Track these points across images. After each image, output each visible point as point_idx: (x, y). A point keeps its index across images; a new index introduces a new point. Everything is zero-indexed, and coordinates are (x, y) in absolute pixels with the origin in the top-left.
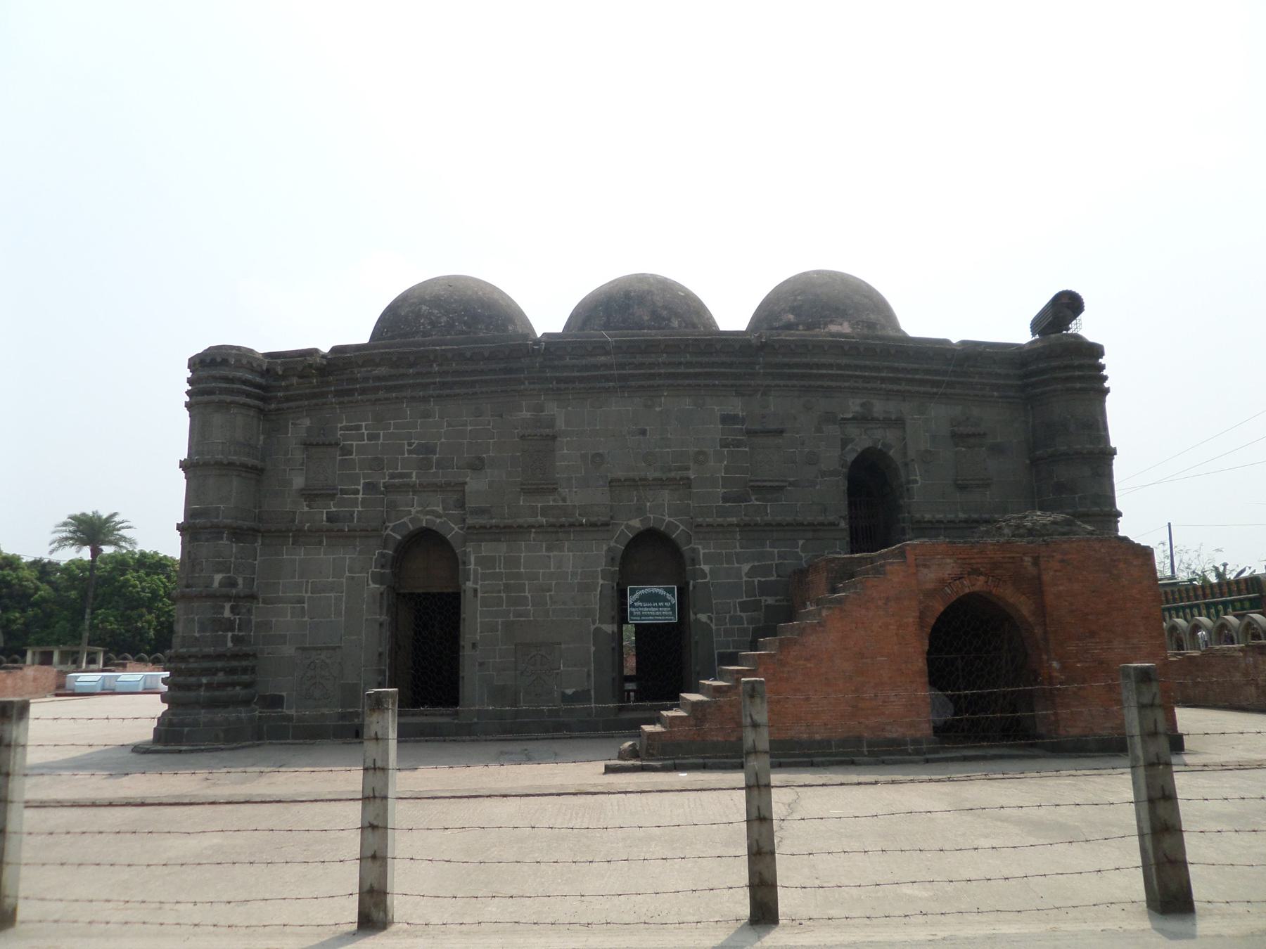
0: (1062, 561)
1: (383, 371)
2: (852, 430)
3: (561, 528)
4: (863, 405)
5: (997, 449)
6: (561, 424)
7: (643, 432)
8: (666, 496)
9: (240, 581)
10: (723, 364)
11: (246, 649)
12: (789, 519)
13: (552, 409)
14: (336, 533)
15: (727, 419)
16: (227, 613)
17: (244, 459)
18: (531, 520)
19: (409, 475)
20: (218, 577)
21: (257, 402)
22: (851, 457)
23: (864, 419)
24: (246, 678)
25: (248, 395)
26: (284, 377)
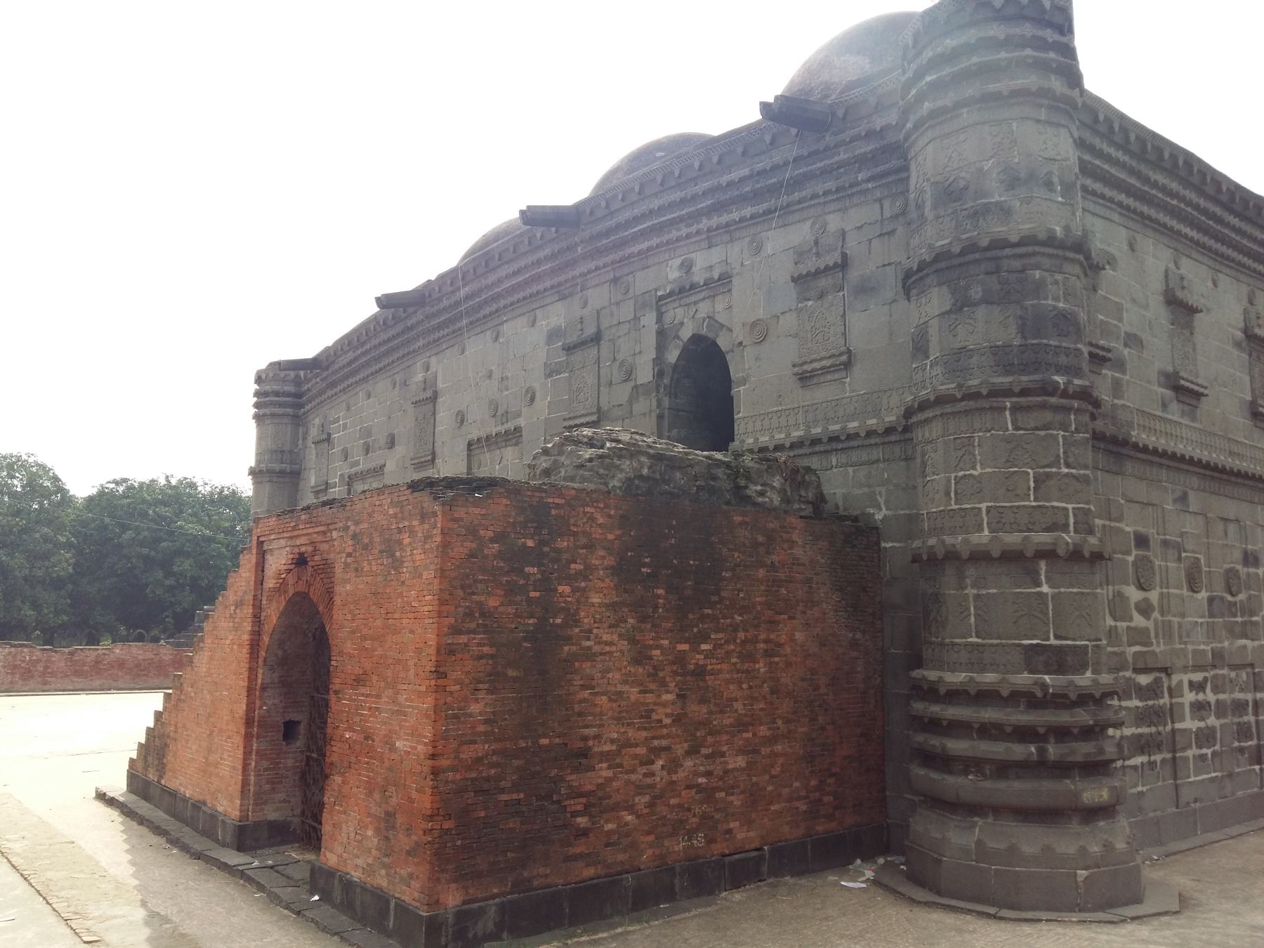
0: (354, 537)
1: (351, 355)
2: (675, 313)
4: (682, 264)
5: (865, 289)
8: (510, 453)
13: (433, 360)
15: (553, 335)
21: (289, 411)
22: (673, 356)
23: (684, 291)
25: (281, 405)
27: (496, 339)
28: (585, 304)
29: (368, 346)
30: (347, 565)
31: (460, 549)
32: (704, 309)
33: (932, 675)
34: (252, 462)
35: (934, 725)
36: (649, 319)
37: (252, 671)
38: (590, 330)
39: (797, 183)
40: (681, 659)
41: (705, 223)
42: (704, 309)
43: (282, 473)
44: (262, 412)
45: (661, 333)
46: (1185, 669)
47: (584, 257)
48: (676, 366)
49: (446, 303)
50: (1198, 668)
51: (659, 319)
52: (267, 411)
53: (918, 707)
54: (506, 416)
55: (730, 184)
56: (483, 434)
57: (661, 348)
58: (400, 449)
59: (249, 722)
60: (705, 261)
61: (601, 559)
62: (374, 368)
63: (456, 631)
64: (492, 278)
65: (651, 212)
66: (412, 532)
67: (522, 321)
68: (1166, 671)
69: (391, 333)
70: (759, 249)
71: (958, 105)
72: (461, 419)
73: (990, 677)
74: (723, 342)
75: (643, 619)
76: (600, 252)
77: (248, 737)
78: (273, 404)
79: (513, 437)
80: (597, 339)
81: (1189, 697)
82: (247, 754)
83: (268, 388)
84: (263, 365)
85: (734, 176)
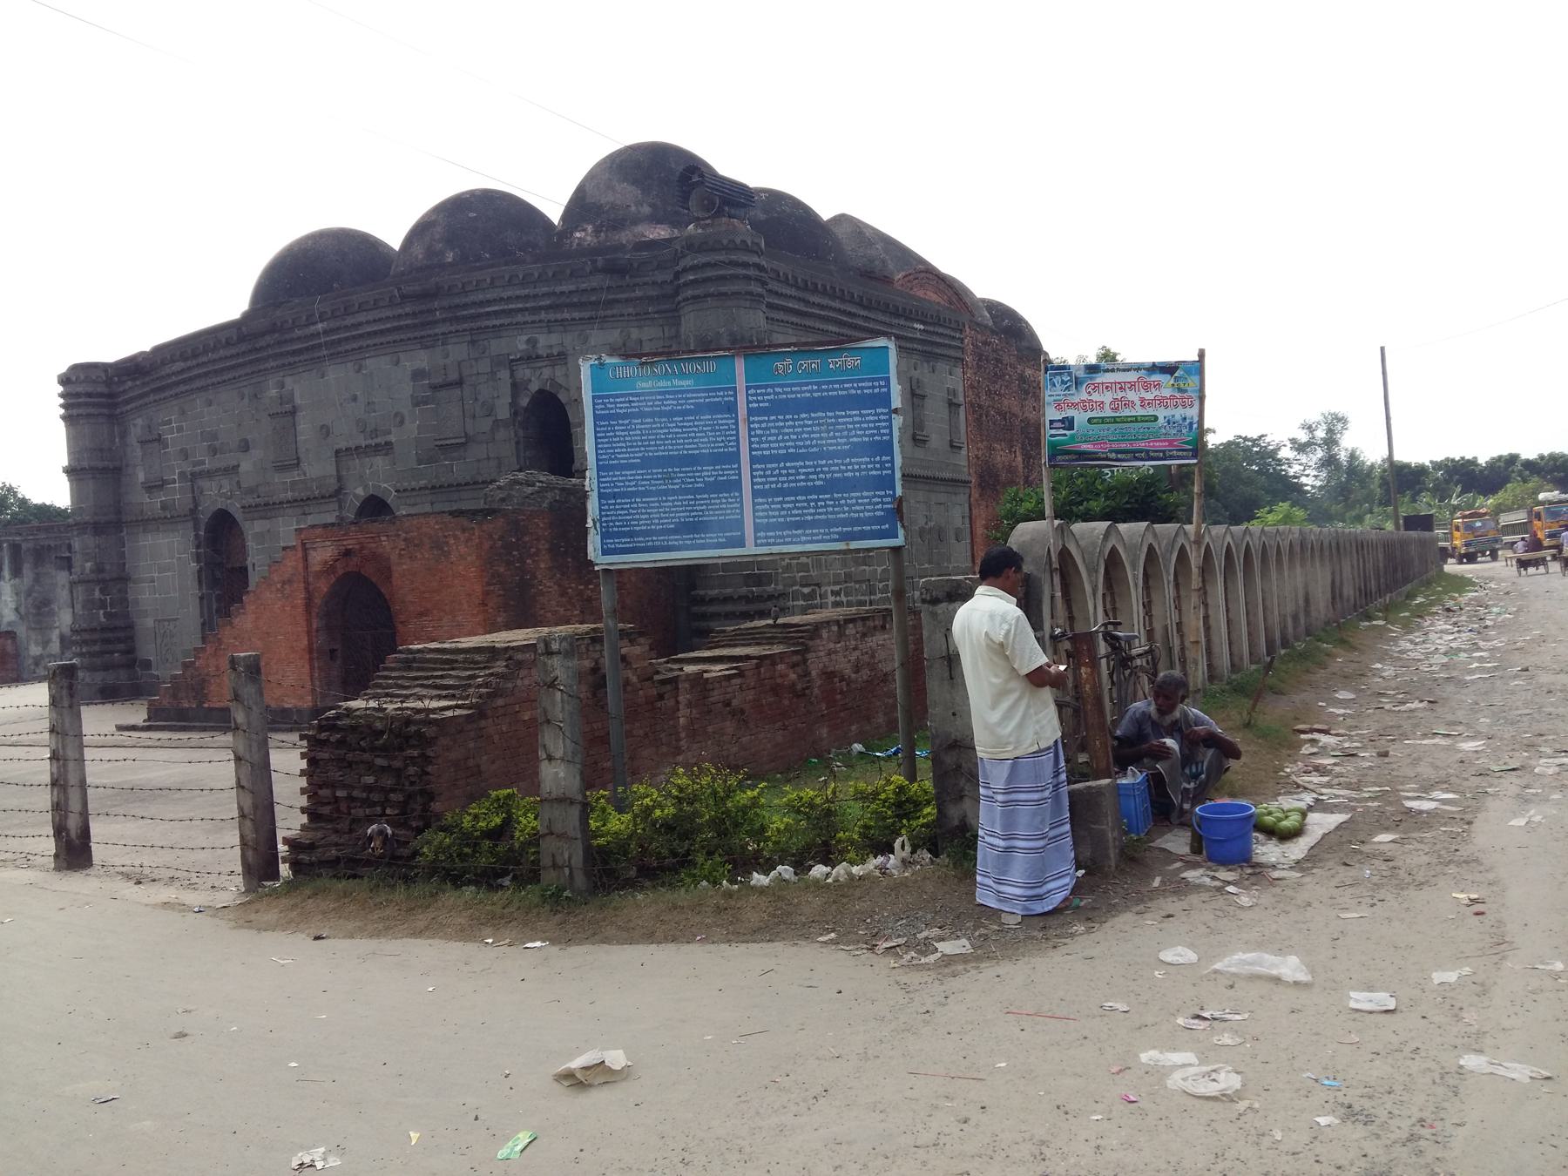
0: (405, 540)
1: (179, 366)
2: (524, 372)
3: (302, 503)
4: (528, 341)
6: (298, 401)
7: (355, 399)
8: (380, 462)
9: (108, 567)
10: (407, 314)
11: (119, 623)
12: (468, 479)
13: (288, 380)
14: (166, 520)
15: (418, 375)
16: (97, 594)
17: (93, 464)
18: (282, 496)
19: (203, 463)
20: (88, 565)
21: (105, 411)
22: (524, 401)
23: (530, 358)
24: (122, 646)
25: (94, 405)
26: (122, 382)
27: (359, 371)
28: (447, 356)
29: (205, 359)
30: (400, 555)
31: (487, 545)
32: (547, 372)
33: (702, 592)
34: (66, 463)
35: (704, 617)
36: (504, 375)
37: (309, 622)
38: (453, 376)
39: (610, 303)
40: (580, 593)
41: (543, 315)
42: (547, 372)
43: (104, 470)
44: (75, 412)
45: (515, 386)
46: (829, 584)
47: (444, 320)
48: (526, 409)
49: (298, 333)
50: (835, 583)
51: (512, 376)
52: (81, 411)
53: (695, 609)
54: (375, 432)
55: (562, 293)
56: (352, 444)
57: (515, 396)
58: (257, 453)
59: (310, 651)
60: (547, 341)
61: (544, 545)
62: (215, 380)
63: (489, 584)
64: (349, 321)
65: (502, 299)
66: (455, 537)
67: (388, 358)
68: (818, 585)
69: (233, 351)
70: (586, 341)
71: (706, 296)
72: (326, 431)
73: (729, 590)
74: (562, 397)
75: (563, 574)
76: (457, 319)
77: (311, 660)
78: (87, 404)
79: (386, 448)
80: (459, 383)
81: (831, 599)
82: (312, 668)
83: (80, 389)
84: (63, 369)
85: (564, 288)
